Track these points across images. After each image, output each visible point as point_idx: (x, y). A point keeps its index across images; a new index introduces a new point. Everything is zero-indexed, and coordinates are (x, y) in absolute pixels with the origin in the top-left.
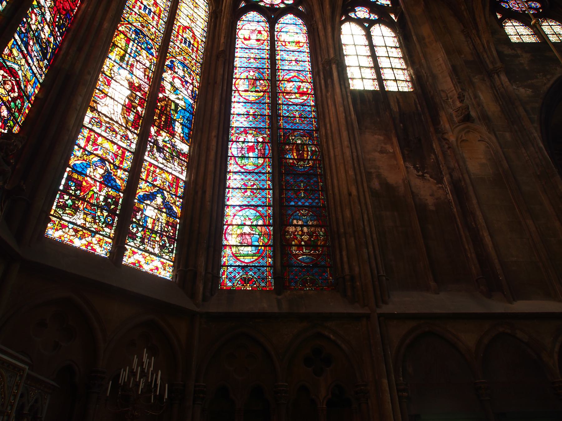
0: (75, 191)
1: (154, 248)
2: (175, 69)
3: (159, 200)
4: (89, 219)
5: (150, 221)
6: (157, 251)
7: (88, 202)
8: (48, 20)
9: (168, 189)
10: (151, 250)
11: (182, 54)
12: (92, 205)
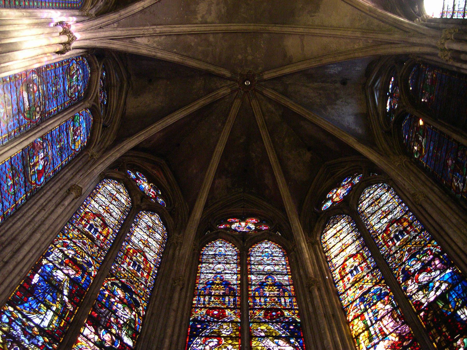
2: (411, 271)
11: (404, 252)
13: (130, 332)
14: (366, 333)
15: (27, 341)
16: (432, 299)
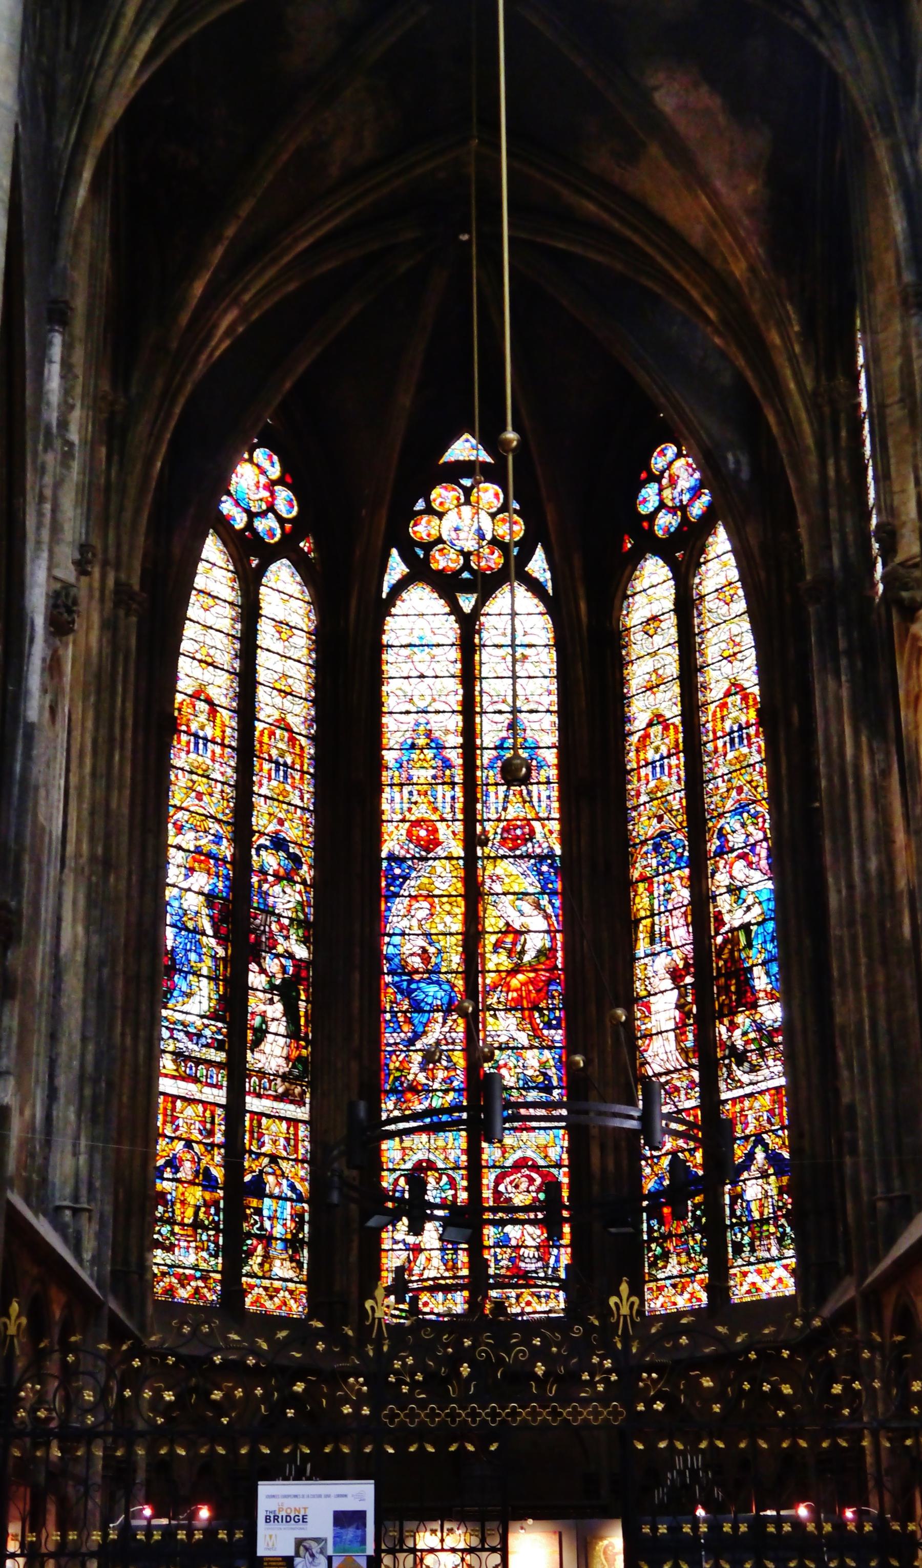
0: (659, 1228)
1: (769, 1250)
2: (728, 841)
3: (760, 1155)
4: (684, 1258)
5: (754, 1206)
6: (775, 1252)
7: (676, 1235)
8: (526, 1043)
9: (768, 1126)
10: (767, 1255)
12: (682, 1235)
13: (301, 932)
14: (649, 920)
15: (196, 1048)
16: (736, 924)
